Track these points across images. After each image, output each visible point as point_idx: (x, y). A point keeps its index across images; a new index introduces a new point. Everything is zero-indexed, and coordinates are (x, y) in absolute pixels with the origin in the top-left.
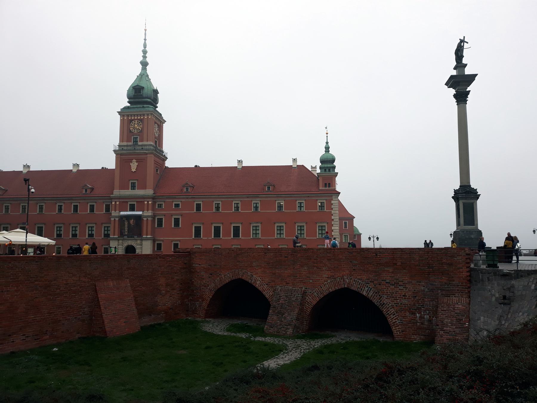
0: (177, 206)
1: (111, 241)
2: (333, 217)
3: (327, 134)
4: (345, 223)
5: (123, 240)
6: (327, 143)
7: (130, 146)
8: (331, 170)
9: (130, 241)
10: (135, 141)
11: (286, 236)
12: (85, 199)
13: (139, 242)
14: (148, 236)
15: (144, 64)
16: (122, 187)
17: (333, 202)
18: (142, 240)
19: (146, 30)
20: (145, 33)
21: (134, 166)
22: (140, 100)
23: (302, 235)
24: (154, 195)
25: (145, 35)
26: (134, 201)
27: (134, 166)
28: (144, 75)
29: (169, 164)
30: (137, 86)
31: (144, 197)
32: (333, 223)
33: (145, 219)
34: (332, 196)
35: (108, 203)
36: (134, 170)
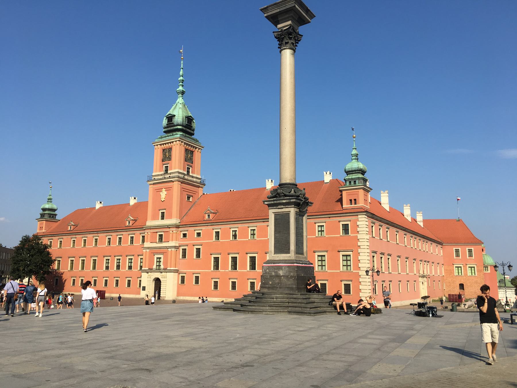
2: (359, 244)
7: (161, 175)
8: (357, 182)
10: (166, 171)
13: (163, 273)
16: (154, 218)
17: (358, 223)
18: (167, 272)
21: (163, 194)
22: (172, 128)
23: (324, 267)
24: (179, 224)
26: (162, 232)
30: (169, 114)
31: (168, 227)
32: (359, 251)
34: (357, 215)
35: (143, 235)
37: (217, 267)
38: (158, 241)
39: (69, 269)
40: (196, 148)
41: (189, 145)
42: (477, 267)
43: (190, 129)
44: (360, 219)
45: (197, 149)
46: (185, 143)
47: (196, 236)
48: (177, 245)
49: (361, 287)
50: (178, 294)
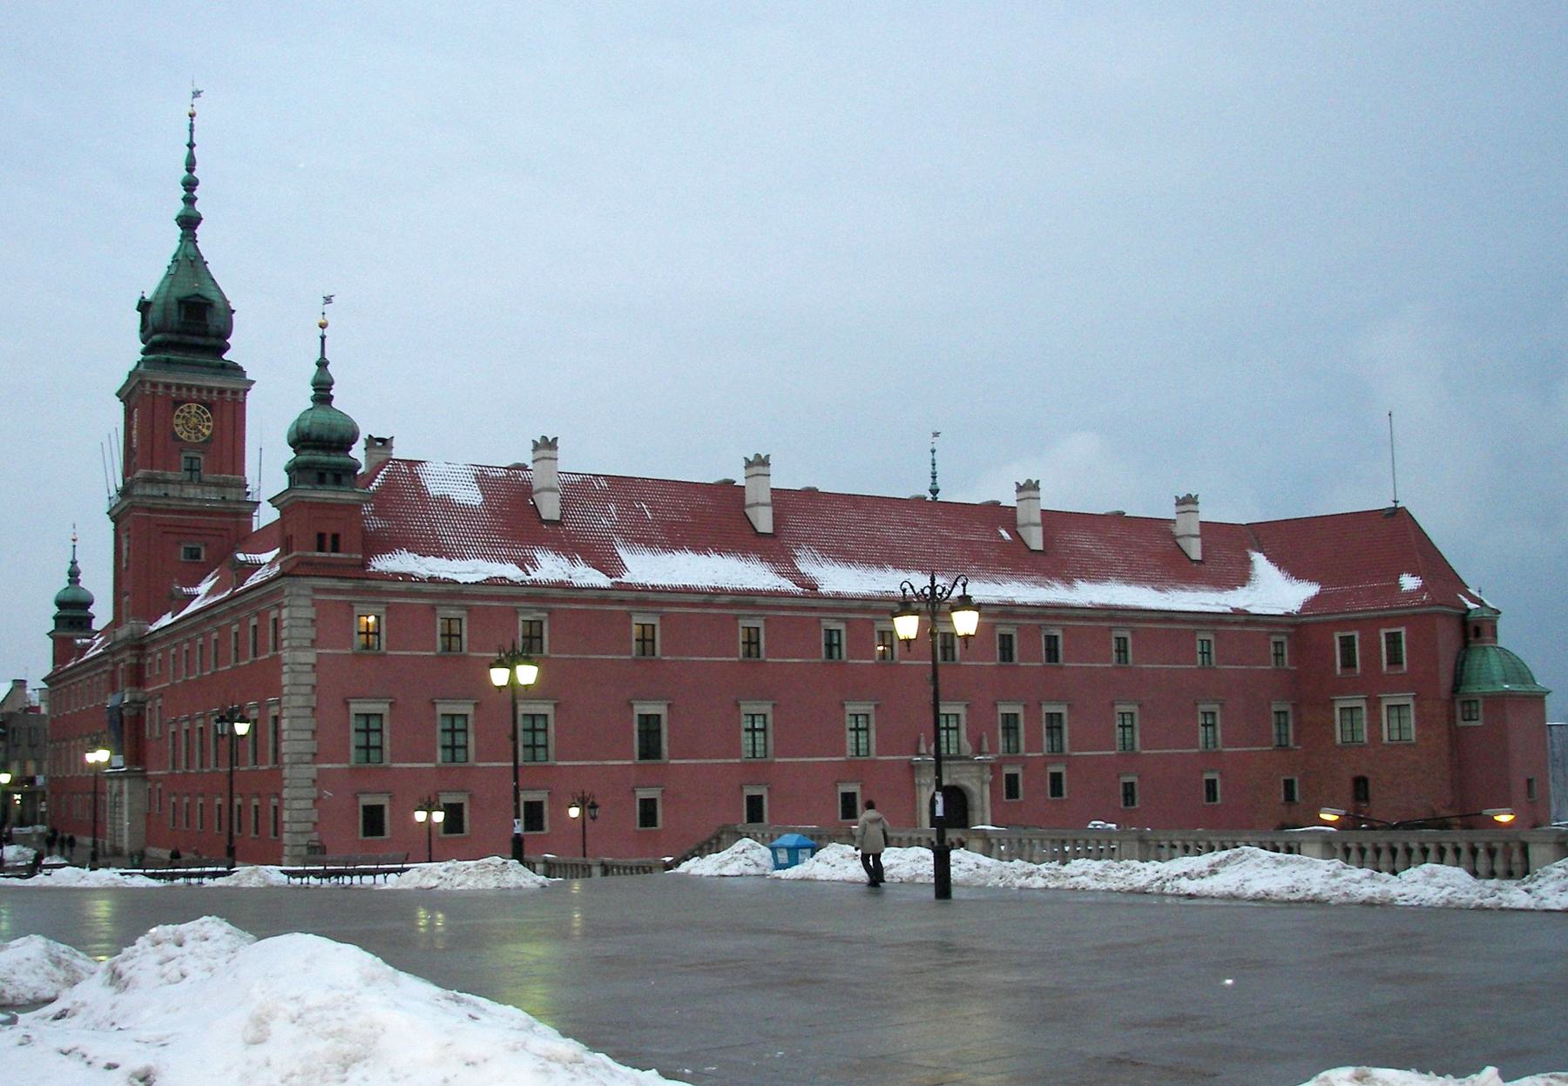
3: (323, 326)
4: (1393, 640)
6: (322, 364)
15: (189, 223)
19: (192, 116)
20: (192, 125)
25: (191, 130)
28: (189, 261)
40: (222, 391)
41: (189, 388)
42: (1418, 706)
43: (206, 334)
45: (229, 394)
46: (168, 386)
48: (139, 696)
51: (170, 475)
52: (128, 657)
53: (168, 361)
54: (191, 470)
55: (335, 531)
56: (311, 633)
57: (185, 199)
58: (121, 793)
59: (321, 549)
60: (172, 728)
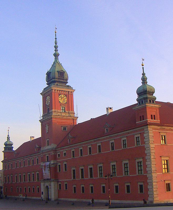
0: (65, 153)
1: (41, 183)
5: (44, 182)
6: (144, 74)
9: (47, 183)
11: (118, 175)
12: (35, 155)
14: (53, 179)
15: (56, 55)
16: (44, 145)
18: (51, 182)
19: (56, 32)
21: (47, 128)
22: (51, 81)
27: (47, 128)
29: (79, 121)
33: (51, 166)
34: (143, 129)
36: (47, 132)
37: (74, 177)
38: (46, 161)
39: (16, 182)
40: (68, 92)
43: (63, 79)
44: (145, 132)
47: (64, 156)
48: (55, 162)
49: (149, 187)
50: (59, 197)
51: (59, 111)
52: (52, 153)
53: (57, 85)
54: (63, 110)
55: (143, 115)
56: (153, 140)
57: (55, 50)
58: (50, 186)
59: (152, 119)
60: (73, 169)
